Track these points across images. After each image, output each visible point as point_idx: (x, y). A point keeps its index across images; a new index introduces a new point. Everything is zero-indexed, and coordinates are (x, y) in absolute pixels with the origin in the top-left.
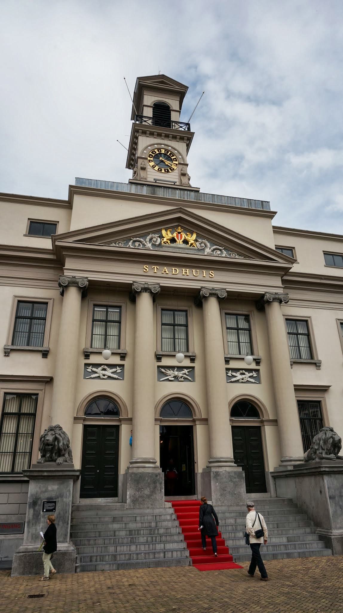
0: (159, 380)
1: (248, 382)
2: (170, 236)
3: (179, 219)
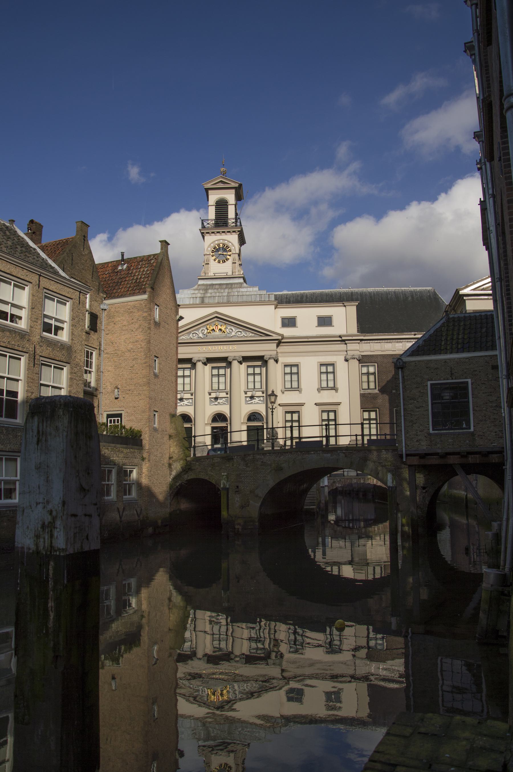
0: (210, 405)
1: (257, 403)
2: (212, 328)
3: (216, 317)
